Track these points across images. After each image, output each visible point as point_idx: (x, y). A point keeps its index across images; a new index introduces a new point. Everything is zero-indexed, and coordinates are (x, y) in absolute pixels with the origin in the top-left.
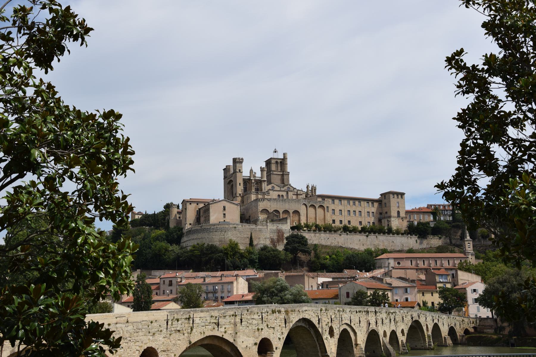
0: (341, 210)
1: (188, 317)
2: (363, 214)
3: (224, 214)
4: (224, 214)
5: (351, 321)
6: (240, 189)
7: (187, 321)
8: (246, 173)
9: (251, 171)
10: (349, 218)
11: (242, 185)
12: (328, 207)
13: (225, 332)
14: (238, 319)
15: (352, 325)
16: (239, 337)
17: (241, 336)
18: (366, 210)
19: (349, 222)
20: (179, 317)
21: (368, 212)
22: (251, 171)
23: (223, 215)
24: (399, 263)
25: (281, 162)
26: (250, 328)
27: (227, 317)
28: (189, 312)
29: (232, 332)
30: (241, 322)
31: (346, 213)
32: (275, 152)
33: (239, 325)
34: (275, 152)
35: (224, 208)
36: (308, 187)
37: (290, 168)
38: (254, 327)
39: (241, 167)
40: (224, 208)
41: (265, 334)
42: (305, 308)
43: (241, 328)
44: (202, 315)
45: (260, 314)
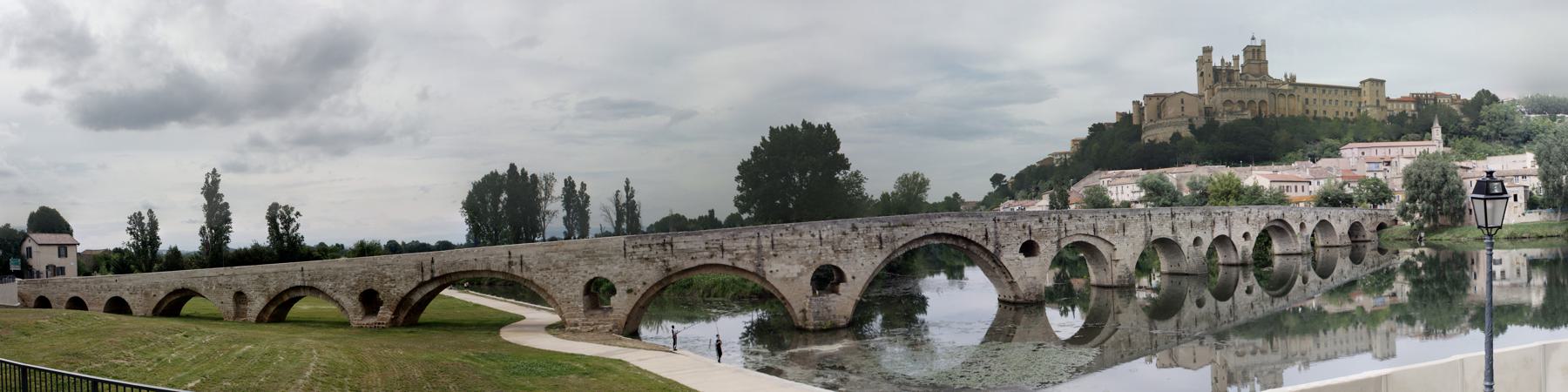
0: (1315, 100)
2: (1340, 104)
3: (1183, 108)
4: (1183, 108)
5: (1094, 231)
6: (1209, 80)
8: (1216, 62)
9: (1223, 60)
10: (1324, 108)
11: (1212, 76)
12: (1298, 96)
15: (1100, 235)
18: (1345, 99)
19: (1325, 112)
21: (1346, 101)
22: (1223, 60)
23: (1180, 109)
24: (1363, 153)
25: (1258, 50)
31: (1321, 102)
32: (1253, 39)
34: (1253, 39)
35: (1182, 102)
36: (1286, 76)
37: (1269, 56)
39: (1211, 57)
40: (1182, 102)
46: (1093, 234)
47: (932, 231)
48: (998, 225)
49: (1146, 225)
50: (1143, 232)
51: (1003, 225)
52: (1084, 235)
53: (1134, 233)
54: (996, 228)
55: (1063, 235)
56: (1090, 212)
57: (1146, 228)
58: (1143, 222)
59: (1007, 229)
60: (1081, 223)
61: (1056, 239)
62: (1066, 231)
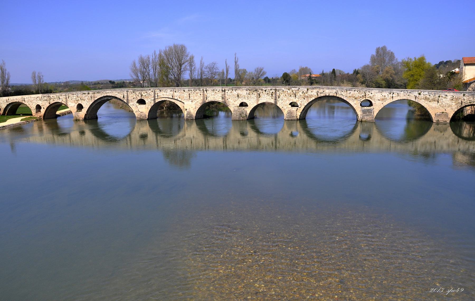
1: (48, 96)
5: (172, 96)
7: (48, 97)
13: (62, 101)
14: (67, 97)
16: (68, 103)
17: (69, 103)
20: (45, 96)
26: (73, 100)
27: (62, 96)
28: (49, 95)
29: (65, 101)
30: (69, 98)
33: (68, 98)
38: (74, 100)
41: (80, 102)
42: (108, 92)
43: (69, 100)
44: (53, 95)
45: (77, 94)
46: (172, 98)
47: (106, 95)
48: (128, 93)
49: (204, 95)
50: (202, 98)
51: (130, 93)
52: (167, 98)
53: (195, 98)
54: (127, 94)
55: (157, 97)
56: (170, 89)
57: (204, 96)
58: (202, 94)
59: (132, 95)
60: (165, 93)
61: (153, 99)
62: (158, 96)
